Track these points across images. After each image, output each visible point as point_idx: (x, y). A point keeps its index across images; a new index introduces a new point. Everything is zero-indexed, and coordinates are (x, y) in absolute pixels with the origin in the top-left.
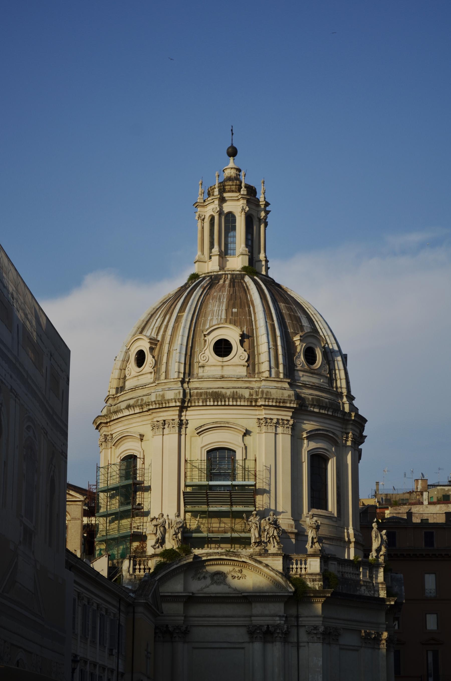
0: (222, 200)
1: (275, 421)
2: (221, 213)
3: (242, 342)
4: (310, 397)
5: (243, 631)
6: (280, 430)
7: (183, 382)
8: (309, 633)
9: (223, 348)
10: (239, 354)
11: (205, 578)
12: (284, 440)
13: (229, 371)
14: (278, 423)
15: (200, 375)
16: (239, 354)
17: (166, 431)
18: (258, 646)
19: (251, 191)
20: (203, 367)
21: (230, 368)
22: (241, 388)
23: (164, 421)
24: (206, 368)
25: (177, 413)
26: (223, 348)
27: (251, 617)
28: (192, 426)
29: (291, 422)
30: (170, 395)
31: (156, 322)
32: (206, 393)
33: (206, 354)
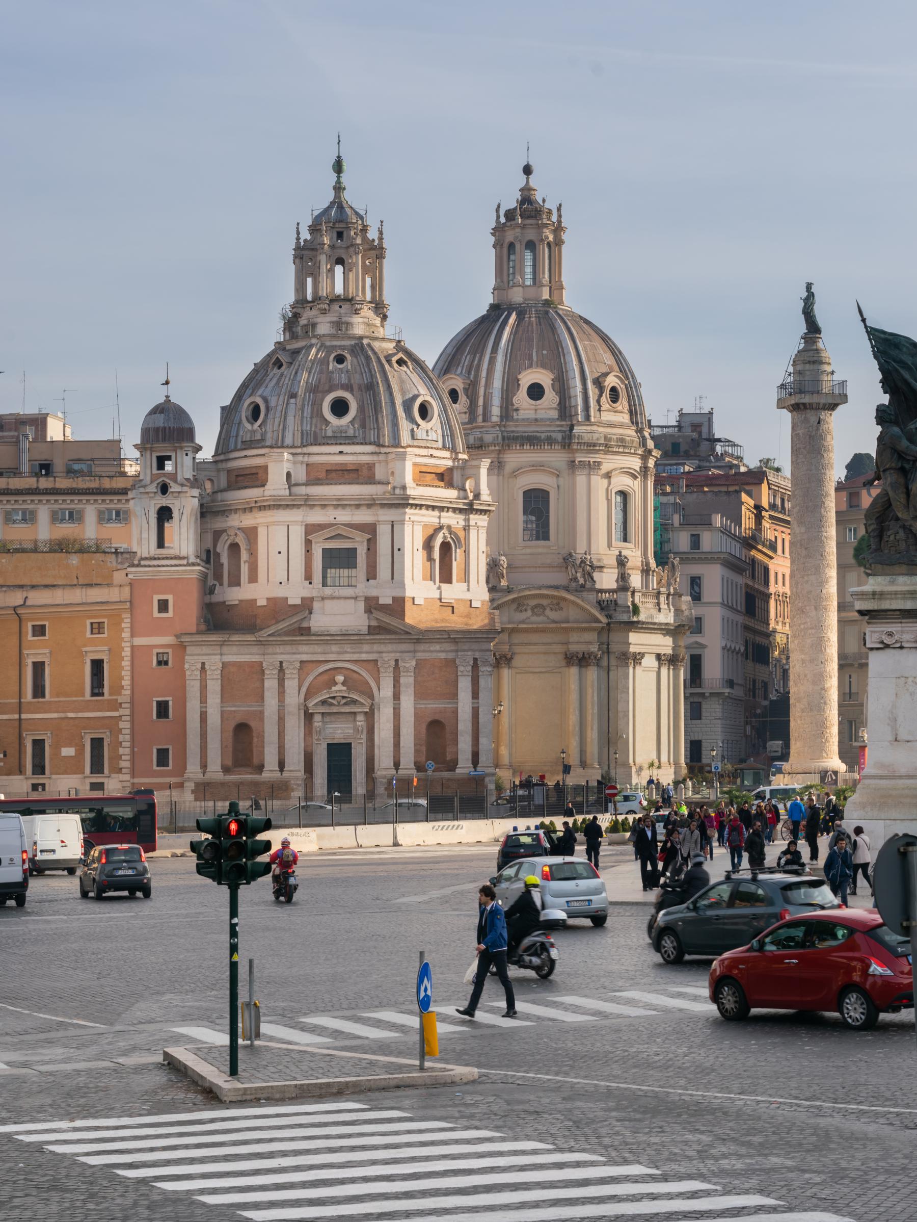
4: (615, 437)
5: (561, 657)
8: (618, 658)
9: (536, 391)
10: (550, 398)
11: (526, 610)
13: (541, 415)
15: (515, 417)
18: (574, 671)
20: (517, 410)
21: (543, 411)
22: (554, 431)
24: (521, 412)
27: (567, 643)
28: (508, 468)
30: (488, 438)
31: (466, 360)
32: (522, 437)
33: (521, 398)
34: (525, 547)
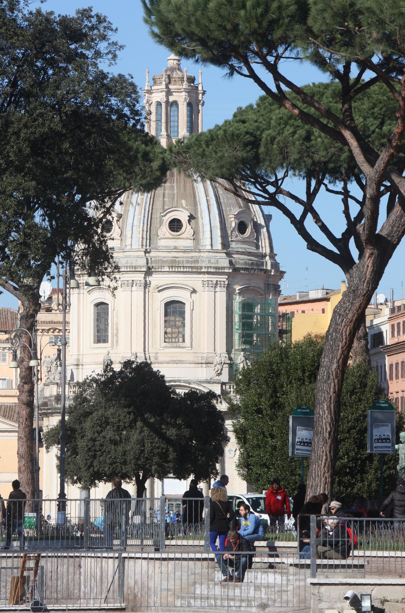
0: (169, 93)
1: (215, 282)
2: (167, 102)
3: (189, 221)
6: (218, 289)
7: (146, 252)
9: (175, 225)
12: (222, 296)
14: (217, 284)
16: (187, 230)
17: (134, 288)
19: (191, 80)
23: (133, 281)
25: (143, 275)
26: (175, 225)
29: (227, 282)
33: (164, 230)
34: (166, 347)
